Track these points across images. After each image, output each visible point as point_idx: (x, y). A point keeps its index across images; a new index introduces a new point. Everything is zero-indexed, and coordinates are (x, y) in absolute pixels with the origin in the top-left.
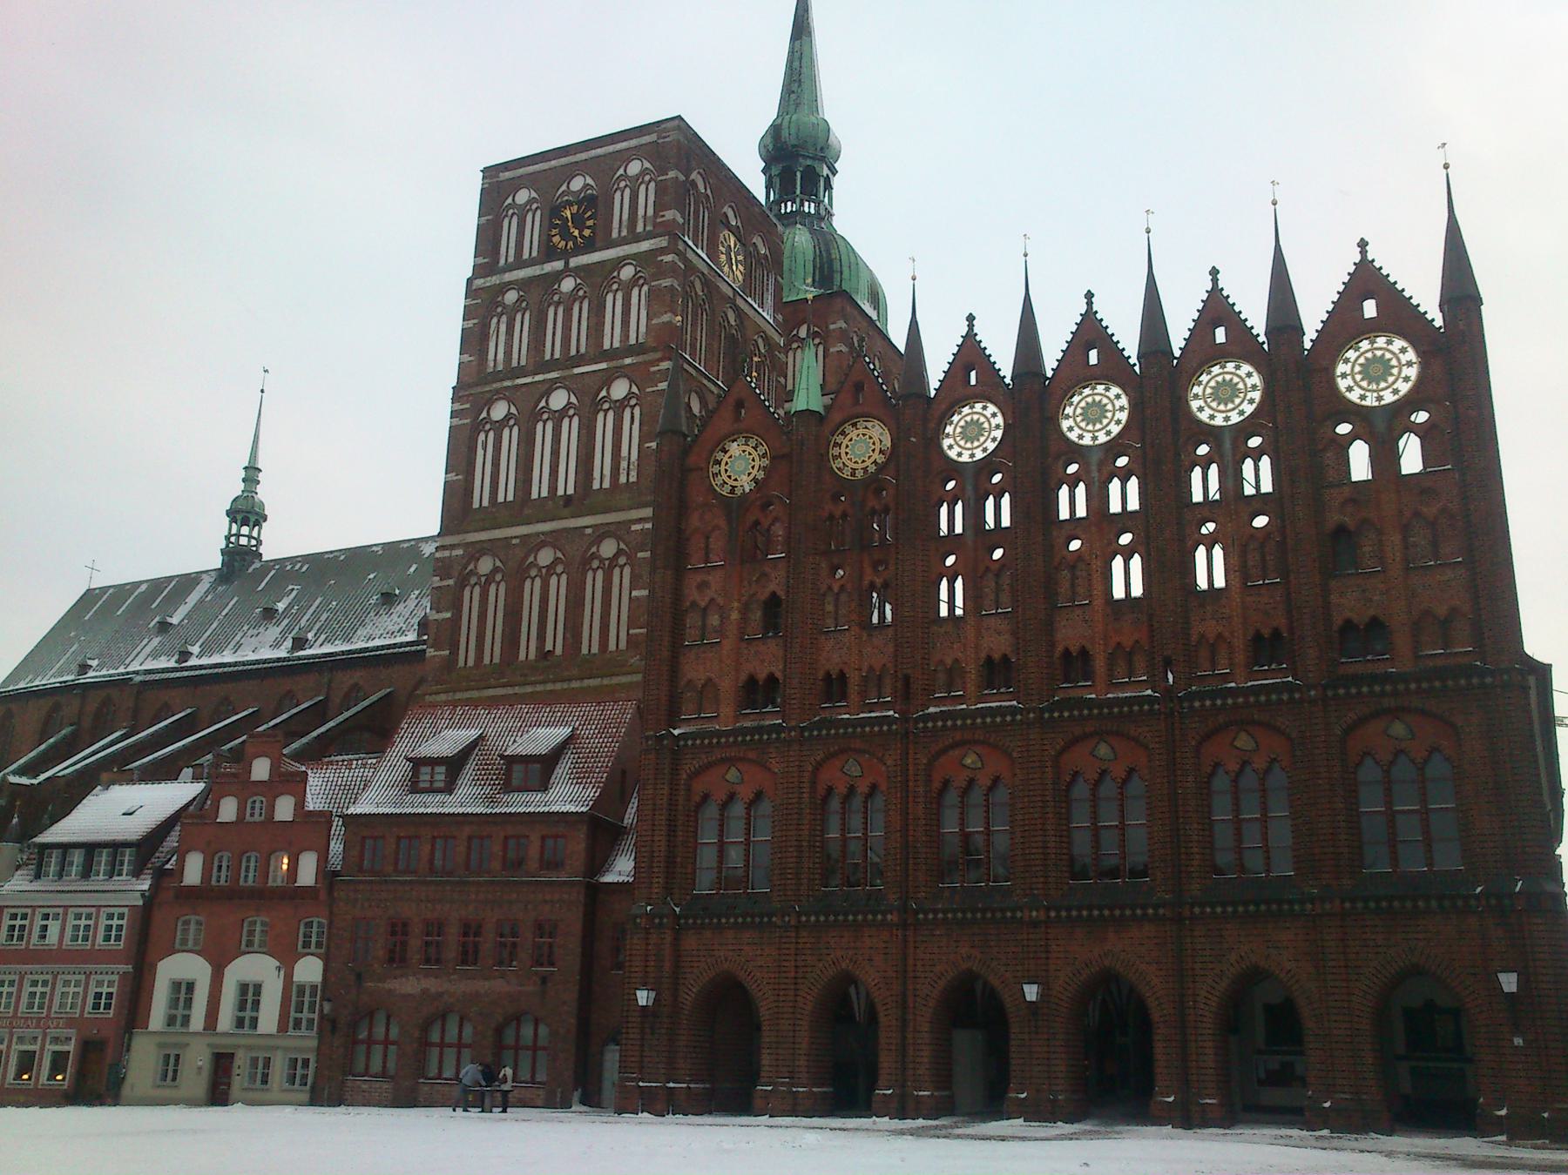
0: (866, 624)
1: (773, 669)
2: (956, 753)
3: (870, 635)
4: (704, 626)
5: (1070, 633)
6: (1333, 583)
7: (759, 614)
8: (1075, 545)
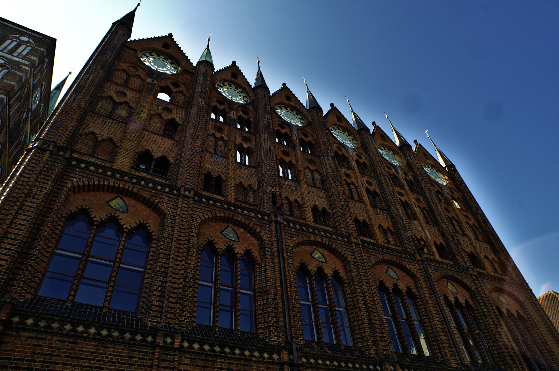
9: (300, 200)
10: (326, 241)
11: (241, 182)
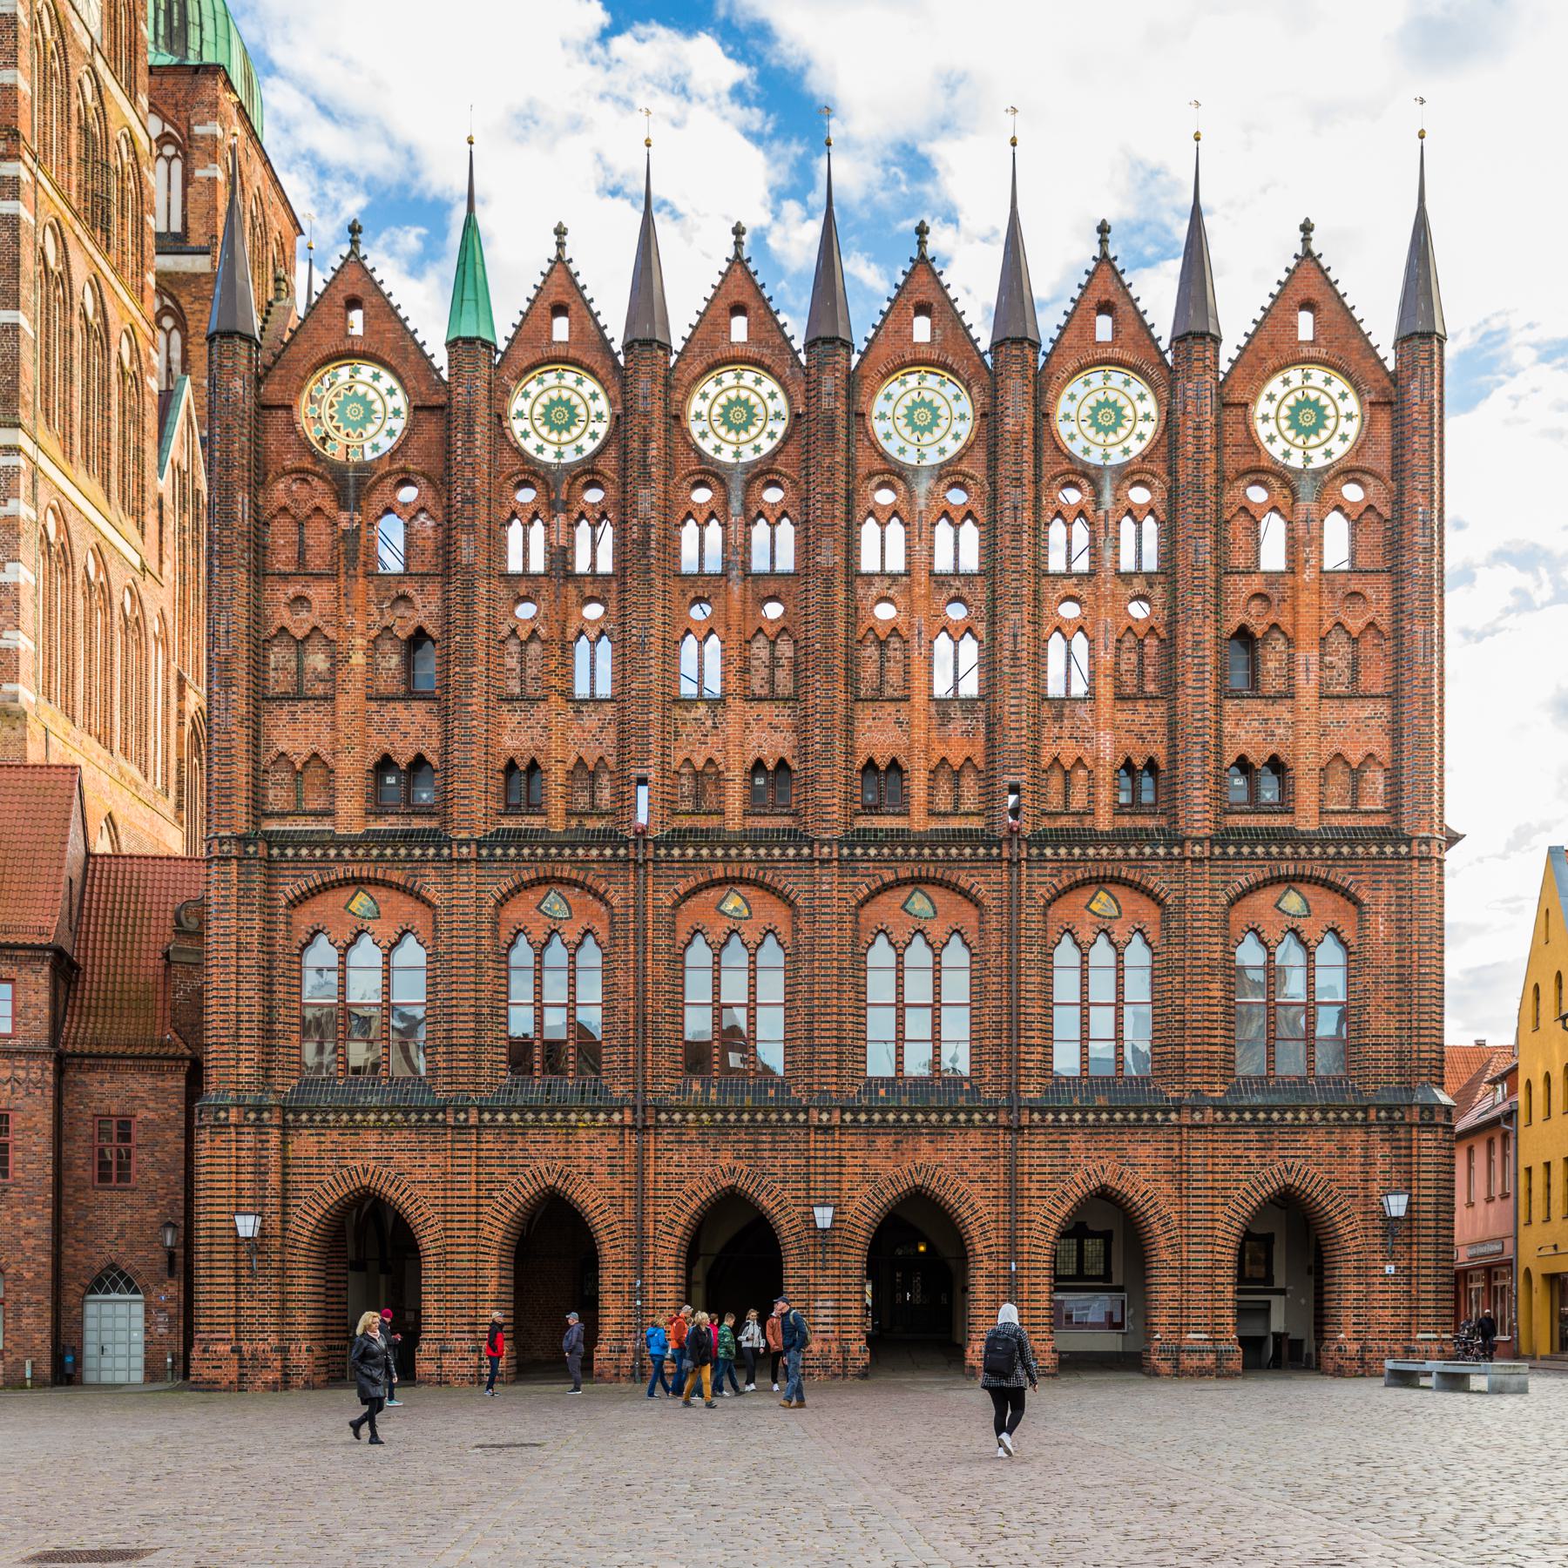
0: (568, 695)
1: (423, 749)
2: (713, 894)
3: (578, 711)
4: (300, 670)
5: (878, 737)
6: (1229, 705)
7: (395, 660)
8: (885, 612)
9: (718, 757)
10: (750, 871)
11: (580, 758)
